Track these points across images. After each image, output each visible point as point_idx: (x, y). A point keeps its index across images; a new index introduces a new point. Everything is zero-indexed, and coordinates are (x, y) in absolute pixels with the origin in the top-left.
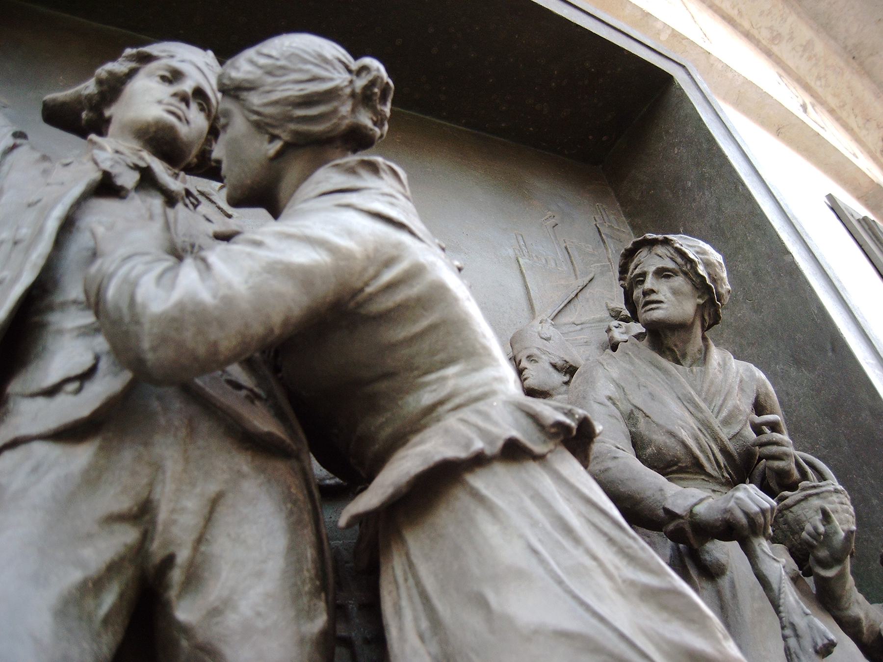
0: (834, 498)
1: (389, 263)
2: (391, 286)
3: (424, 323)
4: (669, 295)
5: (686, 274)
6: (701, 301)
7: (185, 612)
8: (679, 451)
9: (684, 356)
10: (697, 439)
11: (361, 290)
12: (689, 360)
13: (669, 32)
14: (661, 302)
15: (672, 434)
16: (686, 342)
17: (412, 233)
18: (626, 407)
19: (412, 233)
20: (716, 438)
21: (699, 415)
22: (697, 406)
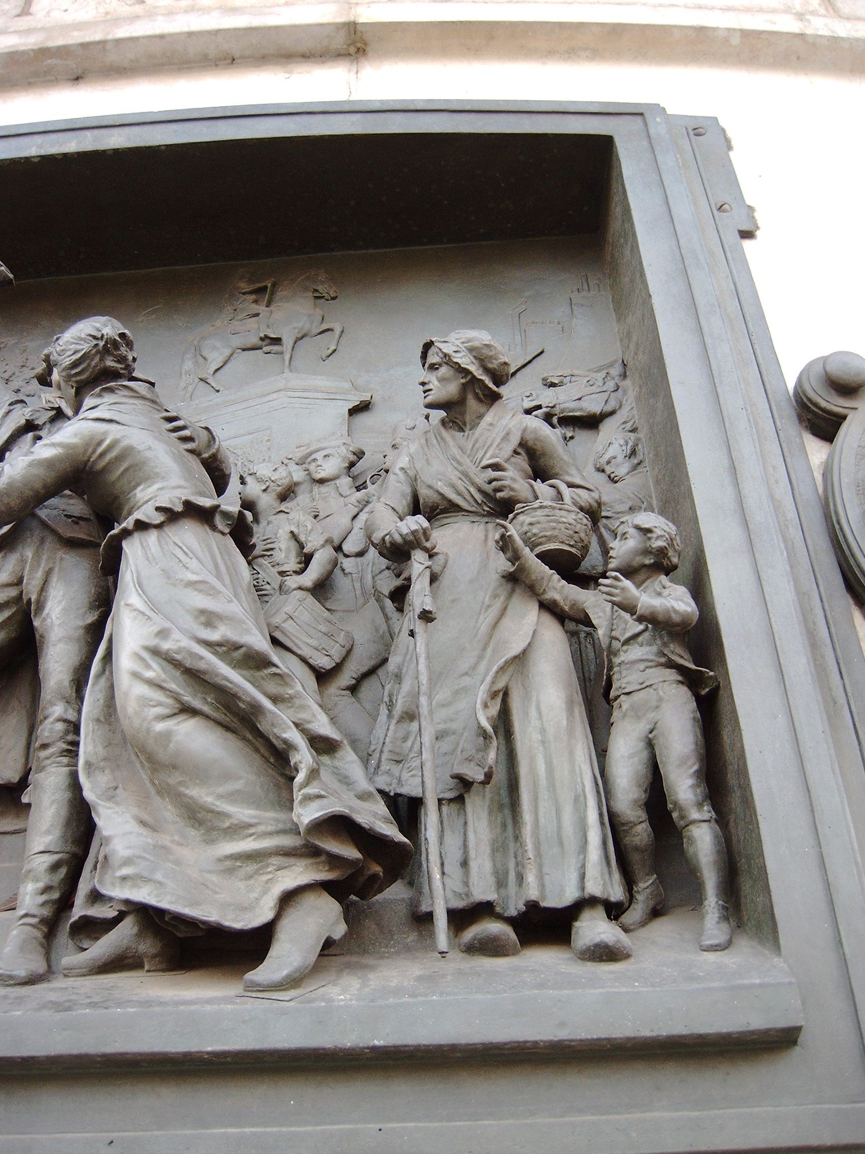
0: (539, 512)
1: (99, 444)
2: (102, 455)
3: (122, 469)
4: (436, 383)
5: (447, 364)
6: (463, 381)
7: (36, 623)
8: (435, 498)
9: (465, 424)
10: (453, 486)
11: (89, 460)
12: (468, 426)
13: (738, 34)
14: (431, 390)
15: (430, 487)
16: (463, 414)
17: (118, 423)
18: (411, 473)
19: (118, 423)
20: (473, 483)
21: (460, 468)
22: (458, 462)
